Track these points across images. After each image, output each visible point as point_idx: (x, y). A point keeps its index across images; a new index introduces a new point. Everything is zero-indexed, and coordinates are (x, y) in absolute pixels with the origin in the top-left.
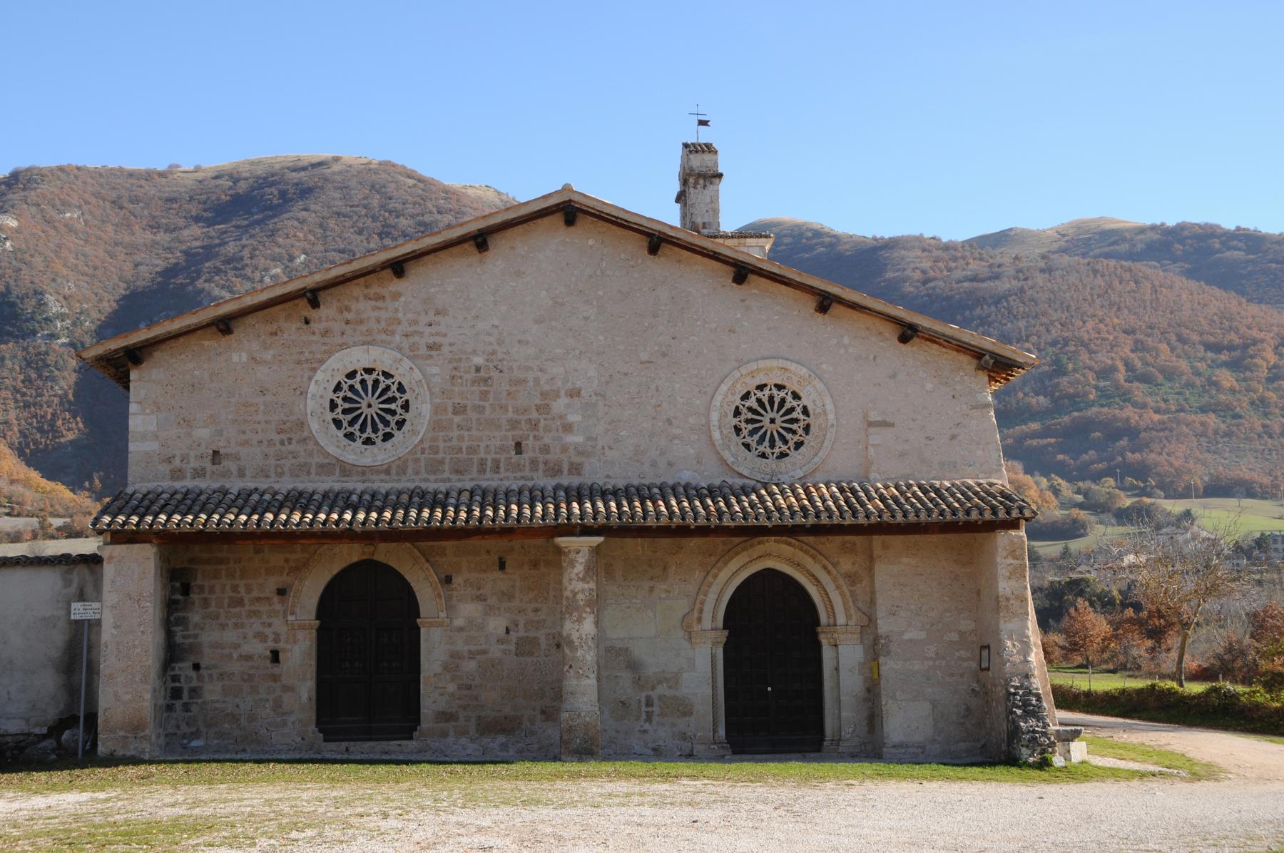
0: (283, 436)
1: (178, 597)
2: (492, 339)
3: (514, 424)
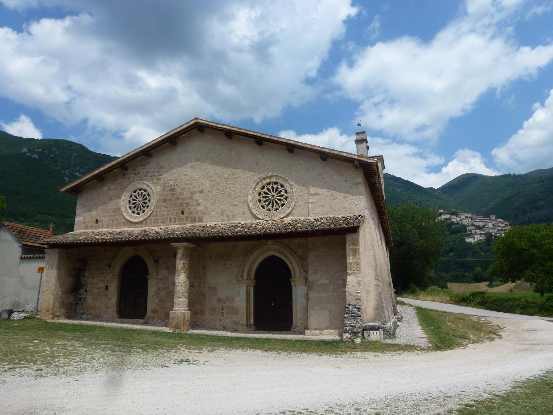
0: (115, 214)
1: (83, 267)
2: (176, 175)
3: (181, 204)
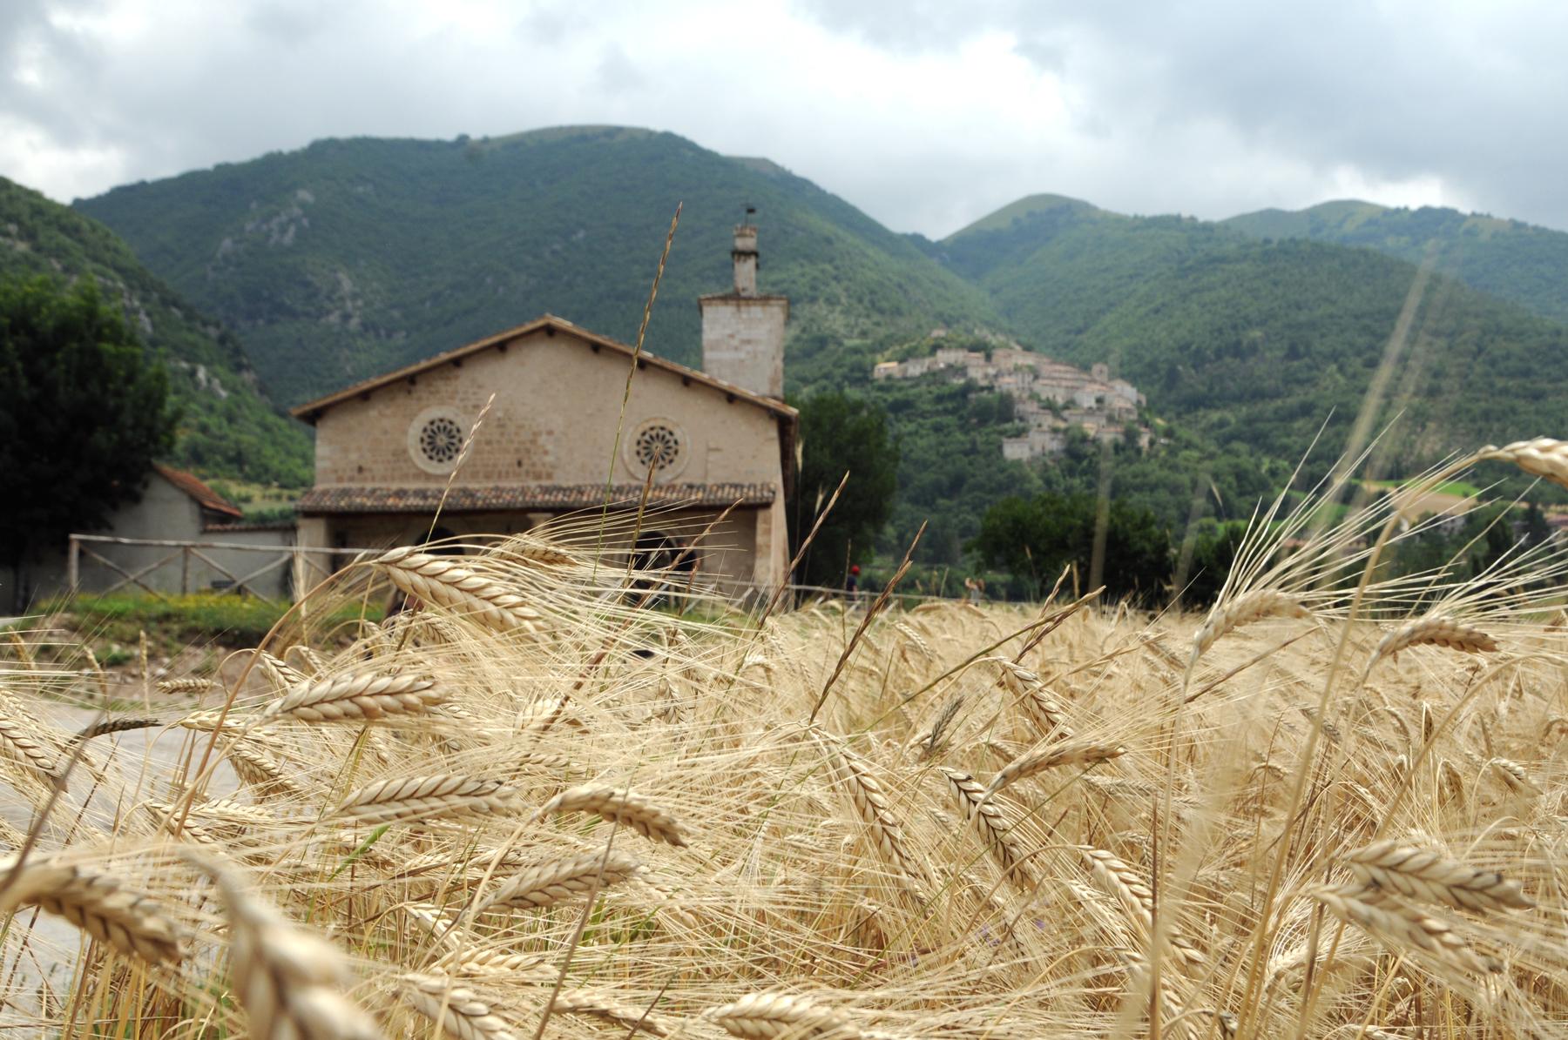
3: (517, 451)
